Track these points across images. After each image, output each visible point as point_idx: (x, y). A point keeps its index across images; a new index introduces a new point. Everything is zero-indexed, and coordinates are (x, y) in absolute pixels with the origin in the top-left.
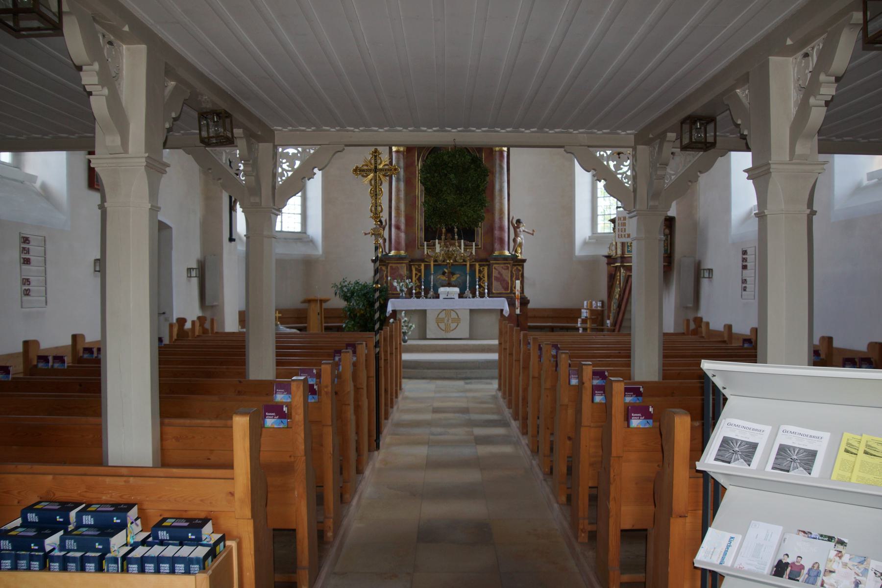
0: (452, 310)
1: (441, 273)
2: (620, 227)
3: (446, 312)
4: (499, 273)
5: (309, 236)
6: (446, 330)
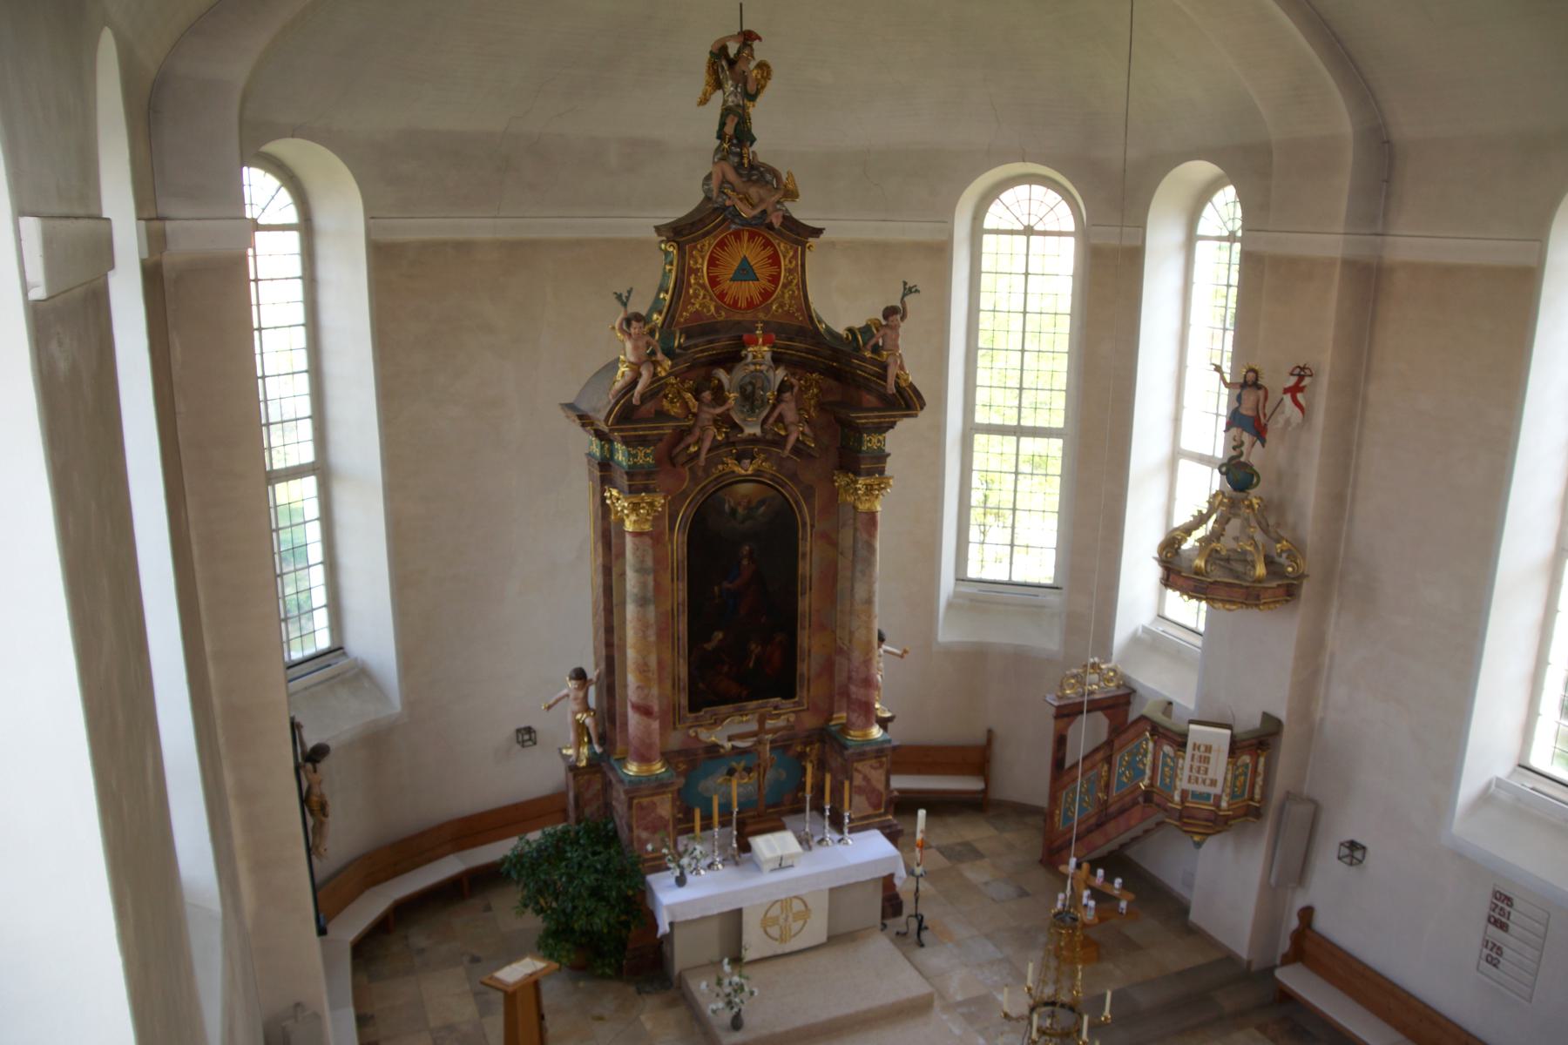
0: (796, 897)
1: (725, 771)
2: (1196, 764)
3: (782, 903)
4: (866, 778)
5: (356, 659)
6: (782, 939)
